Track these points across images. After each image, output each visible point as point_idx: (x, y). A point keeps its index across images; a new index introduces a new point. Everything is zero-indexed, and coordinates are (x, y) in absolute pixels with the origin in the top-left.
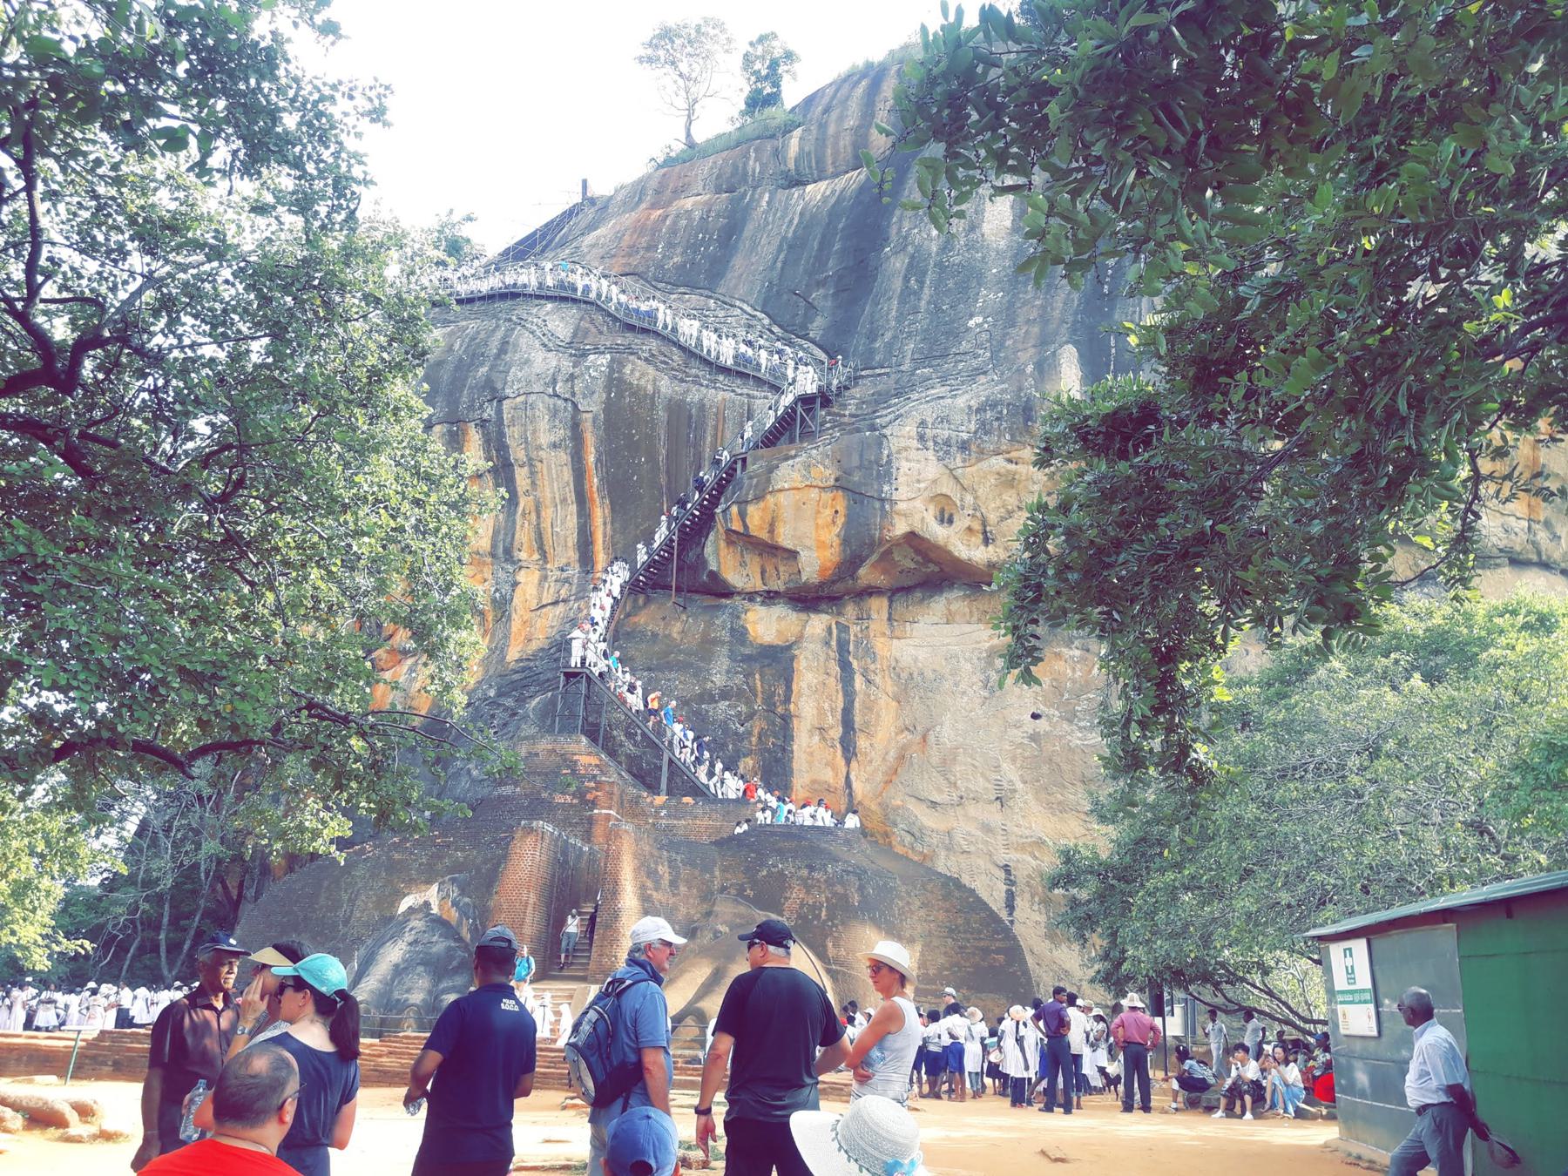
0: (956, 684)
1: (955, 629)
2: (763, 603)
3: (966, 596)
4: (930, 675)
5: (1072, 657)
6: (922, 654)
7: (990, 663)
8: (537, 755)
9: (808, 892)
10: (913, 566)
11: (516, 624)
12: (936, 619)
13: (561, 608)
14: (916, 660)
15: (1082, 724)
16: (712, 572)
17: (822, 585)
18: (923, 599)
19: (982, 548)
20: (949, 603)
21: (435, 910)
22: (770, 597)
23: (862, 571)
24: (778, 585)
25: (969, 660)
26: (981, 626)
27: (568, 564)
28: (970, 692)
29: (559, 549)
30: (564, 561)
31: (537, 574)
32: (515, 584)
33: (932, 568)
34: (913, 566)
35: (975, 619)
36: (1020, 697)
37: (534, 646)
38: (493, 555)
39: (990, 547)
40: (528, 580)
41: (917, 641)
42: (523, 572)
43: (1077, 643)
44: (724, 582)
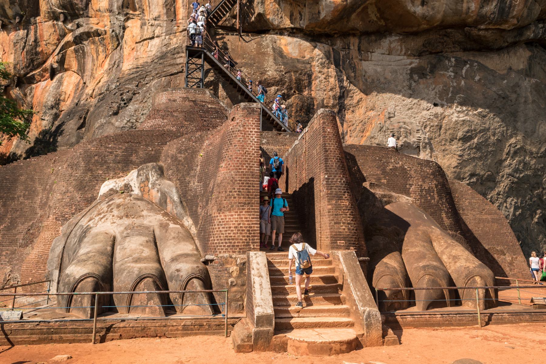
0: (396, 86)
1: (393, 57)
2: (289, 36)
3: (401, 40)
4: (382, 80)
5: (450, 76)
6: (379, 69)
7: (411, 78)
8: (175, 101)
9: (424, 181)
10: (375, 19)
11: (126, 50)
12: (383, 52)
13: (156, 41)
14: (376, 71)
15: (458, 109)
16: (259, 14)
17: (332, 22)
18: (376, 41)
19: (420, 7)
20: (391, 43)
21: (136, 191)
22: (293, 32)
23: (353, 16)
24: (303, 24)
25: (401, 74)
26: (405, 57)
27: (159, 16)
28: (403, 90)
29: (153, 7)
30: (156, 14)
31: (139, 23)
32: (124, 28)
33: (382, 23)
34: (375, 19)
35: (403, 53)
36: (428, 94)
37: (141, 61)
38: (111, 11)
39: (425, 7)
40: (133, 26)
41: (373, 63)
42: (130, 21)
43: (451, 69)
44: (266, 21)
